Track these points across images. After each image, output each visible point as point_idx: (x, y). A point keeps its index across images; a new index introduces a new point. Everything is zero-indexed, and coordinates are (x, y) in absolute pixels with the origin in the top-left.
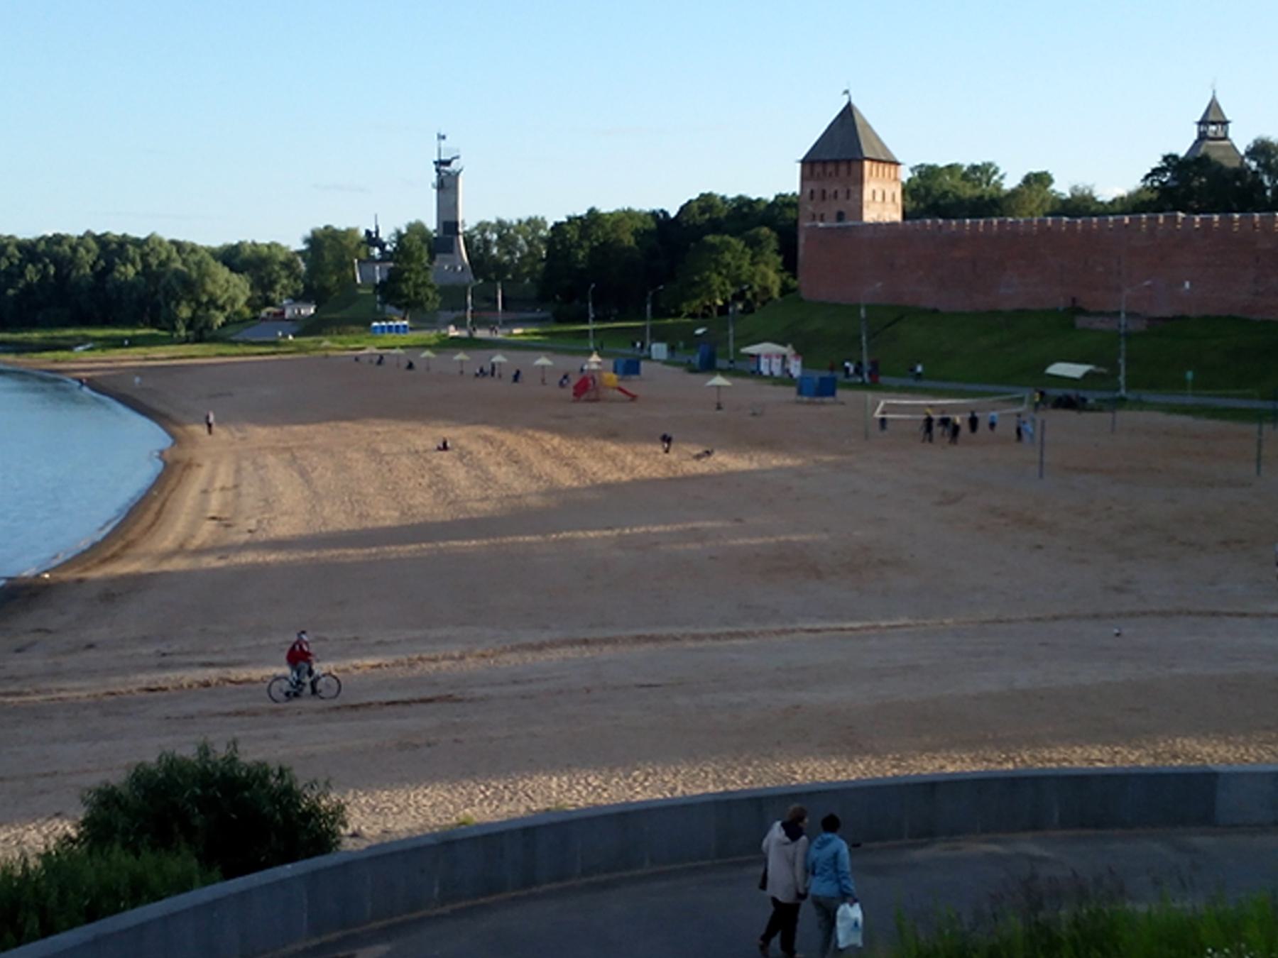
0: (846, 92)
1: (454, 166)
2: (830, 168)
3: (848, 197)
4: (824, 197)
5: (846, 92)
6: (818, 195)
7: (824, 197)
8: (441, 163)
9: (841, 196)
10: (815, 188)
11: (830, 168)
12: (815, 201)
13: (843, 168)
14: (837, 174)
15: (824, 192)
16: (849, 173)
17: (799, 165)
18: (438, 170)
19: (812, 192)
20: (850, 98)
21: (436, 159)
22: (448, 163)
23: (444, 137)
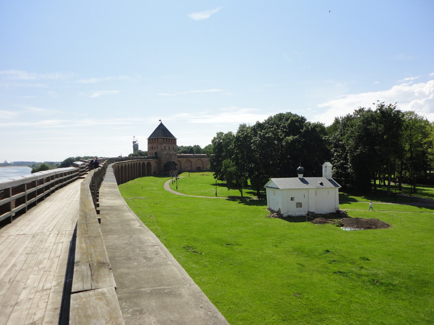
0: (160, 120)
1: (137, 143)
2: (154, 140)
3: (158, 148)
4: (153, 149)
5: (160, 120)
6: (151, 148)
7: (153, 149)
8: (134, 142)
9: (156, 148)
10: (151, 146)
11: (154, 140)
12: (151, 149)
13: (156, 140)
14: (155, 142)
15: (153, 146)
16: (158, 142)
17: (147, 139)
18: (133, 144)
19: (150, 147)
20: (161, 122)
21: (133, 141)
22: (135, 142)
23: (134, 137)
